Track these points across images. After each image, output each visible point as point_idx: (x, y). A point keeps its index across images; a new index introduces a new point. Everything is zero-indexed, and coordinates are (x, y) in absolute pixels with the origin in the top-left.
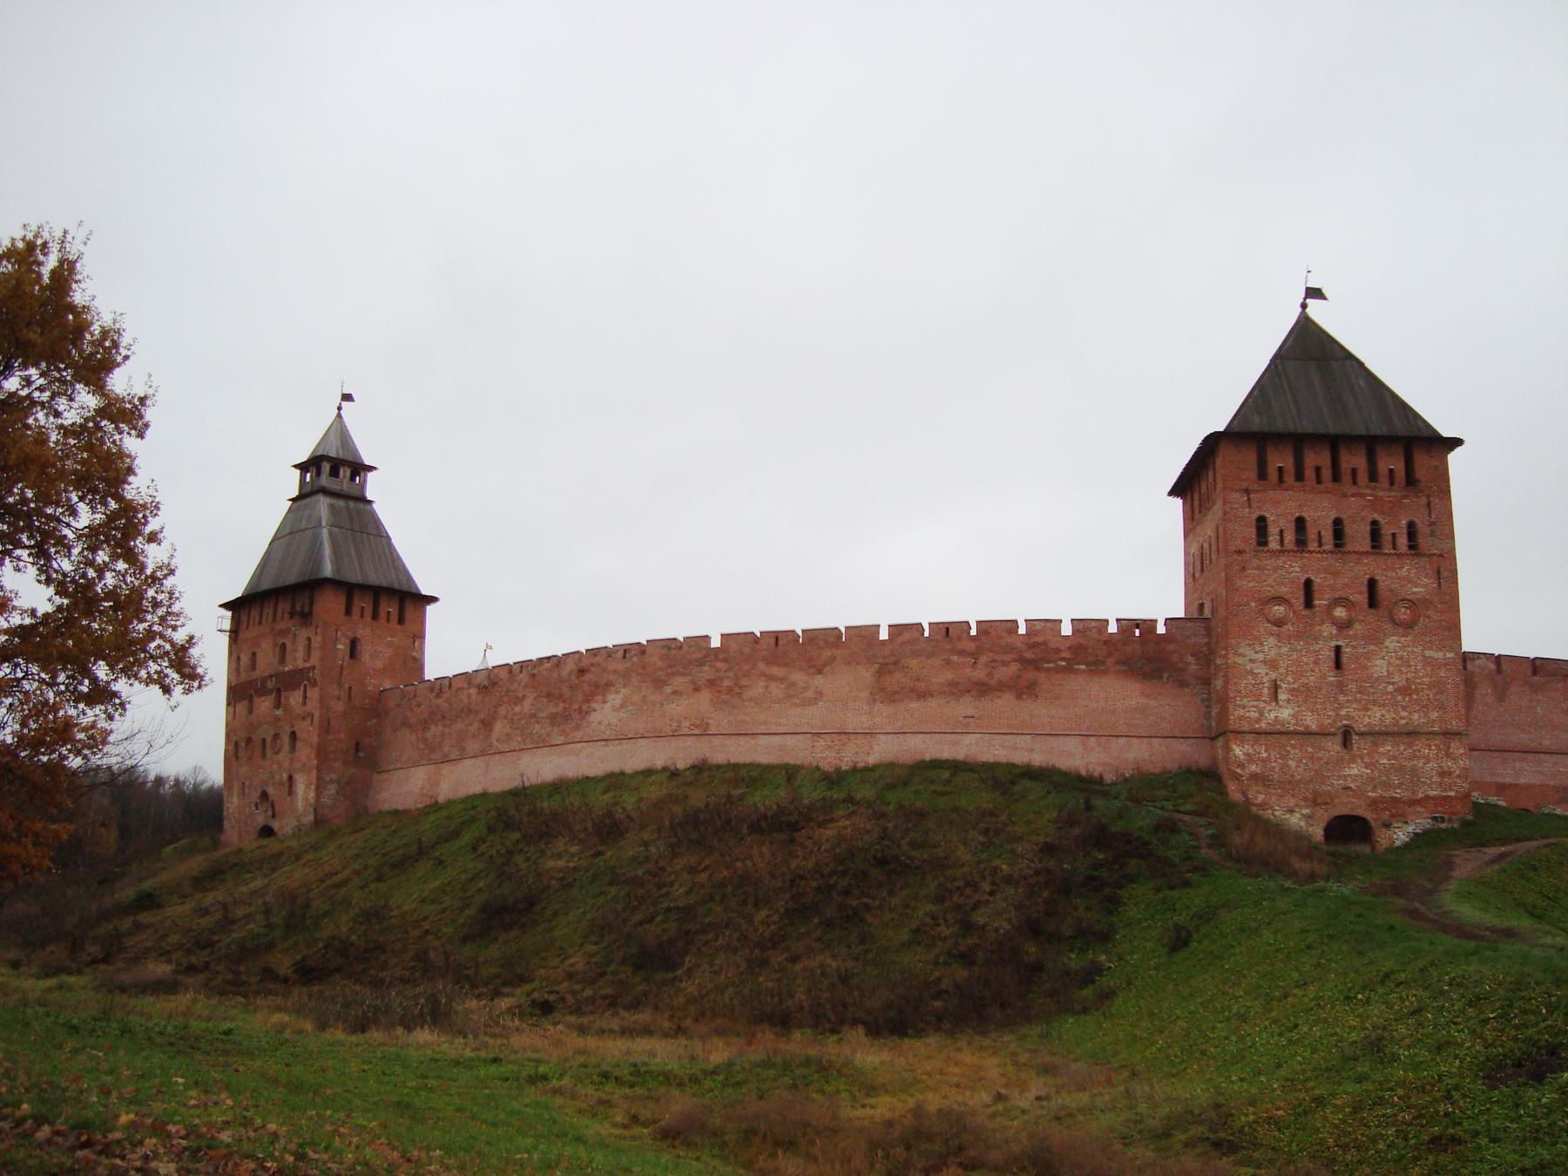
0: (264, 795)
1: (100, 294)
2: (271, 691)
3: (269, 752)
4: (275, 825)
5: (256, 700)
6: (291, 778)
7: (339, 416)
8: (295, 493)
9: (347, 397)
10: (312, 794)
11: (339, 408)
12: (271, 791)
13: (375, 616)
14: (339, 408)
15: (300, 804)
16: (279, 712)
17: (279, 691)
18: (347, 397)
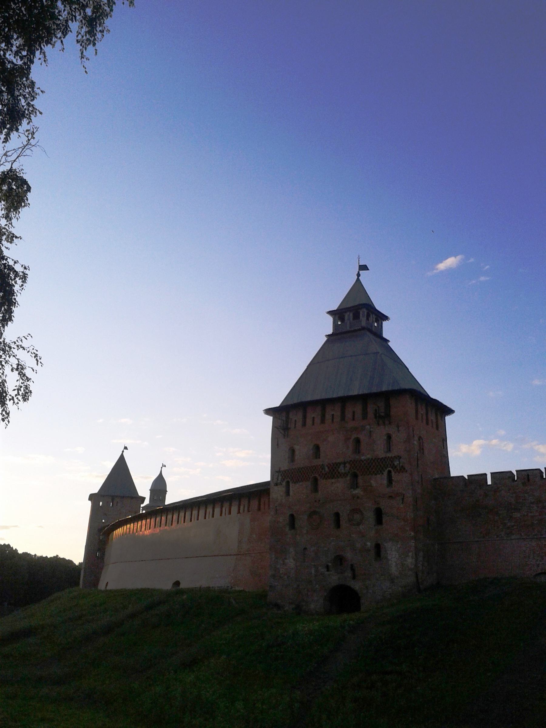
0: (340, 560)
1: (23, 211)
2: (345, 475)
3: (344, 523)
4: (356, 586)
5: (322, 482)
6: (378, 547)
7: (358, 280)
8: (330, 332)
9: (364, 268)
10: (410, 561)
11: (358, 275)
12: (349, 555)
13: (427, 423)
14: (358, 275)
15: (394, 570)
16: (356, 491)
17: (355, 476)
18: (364, 268)
